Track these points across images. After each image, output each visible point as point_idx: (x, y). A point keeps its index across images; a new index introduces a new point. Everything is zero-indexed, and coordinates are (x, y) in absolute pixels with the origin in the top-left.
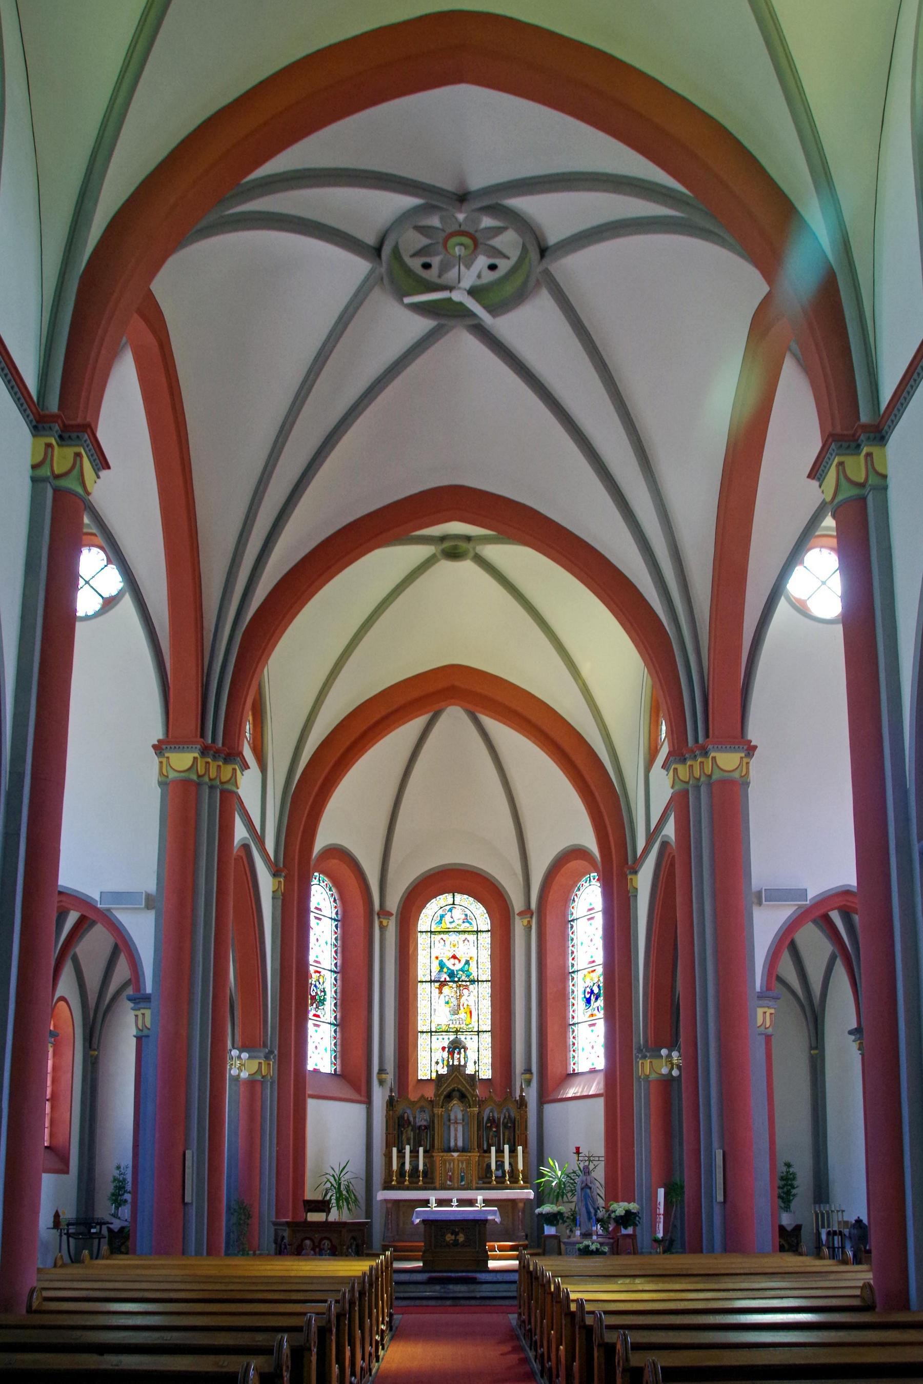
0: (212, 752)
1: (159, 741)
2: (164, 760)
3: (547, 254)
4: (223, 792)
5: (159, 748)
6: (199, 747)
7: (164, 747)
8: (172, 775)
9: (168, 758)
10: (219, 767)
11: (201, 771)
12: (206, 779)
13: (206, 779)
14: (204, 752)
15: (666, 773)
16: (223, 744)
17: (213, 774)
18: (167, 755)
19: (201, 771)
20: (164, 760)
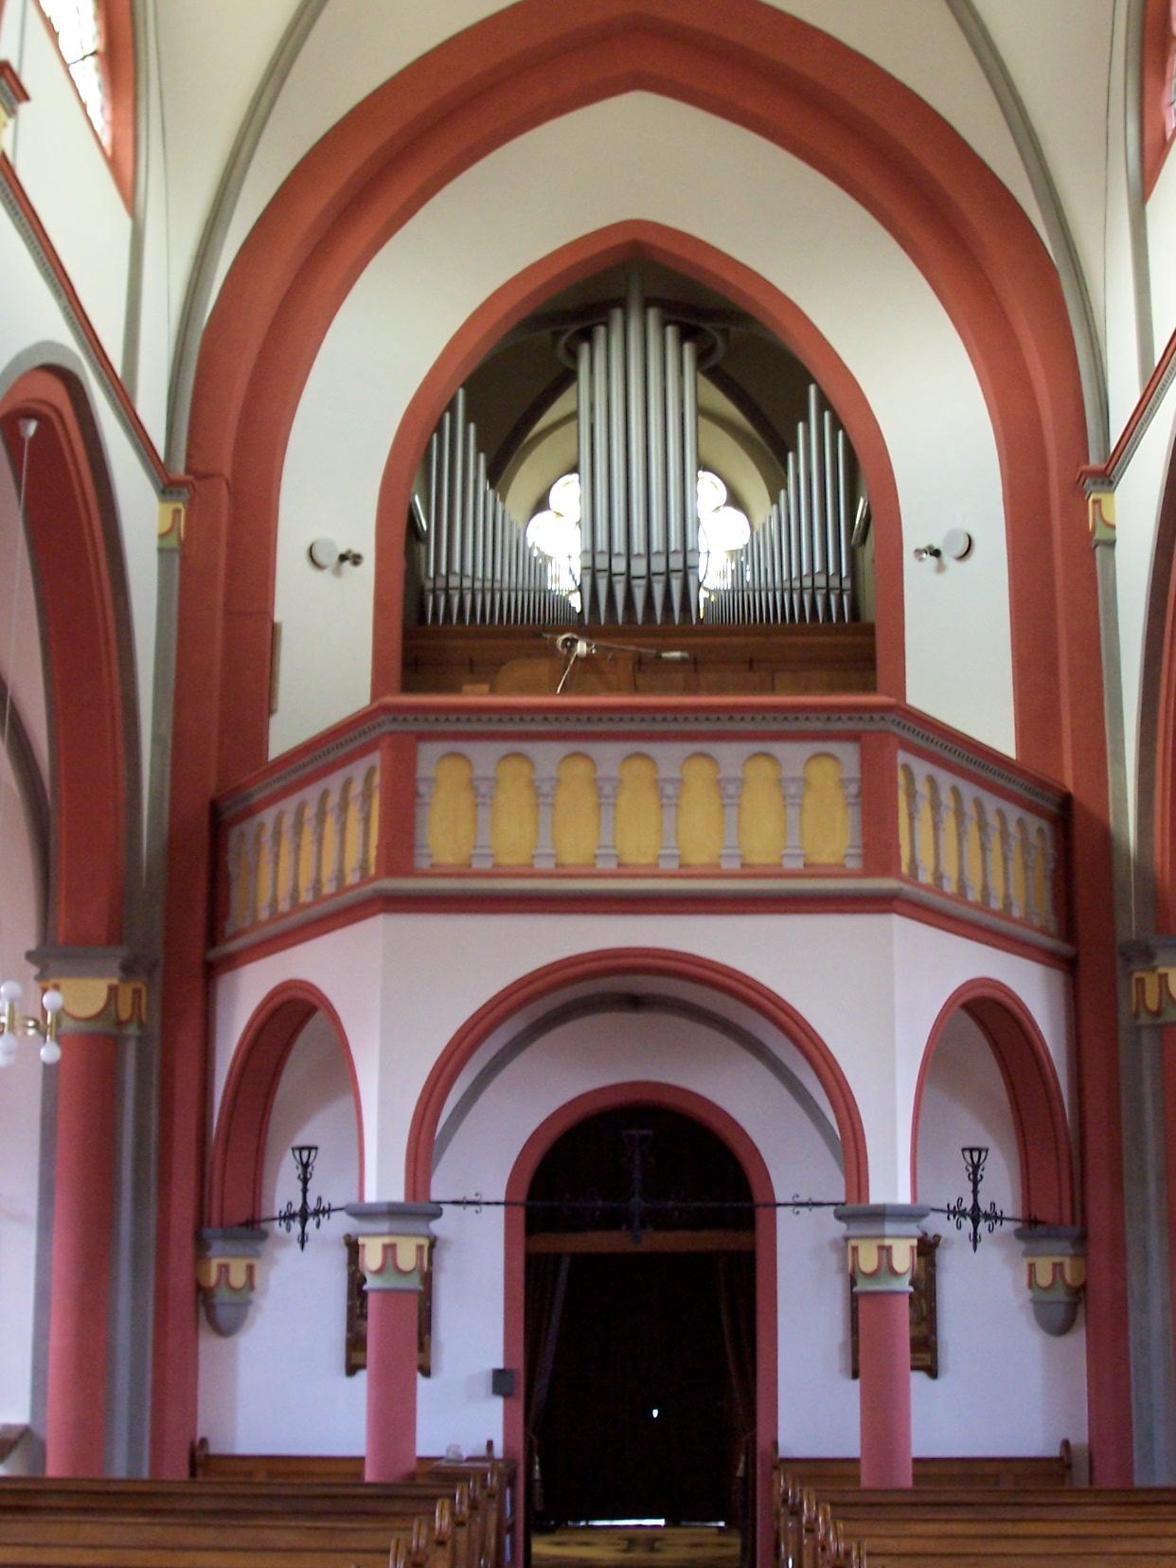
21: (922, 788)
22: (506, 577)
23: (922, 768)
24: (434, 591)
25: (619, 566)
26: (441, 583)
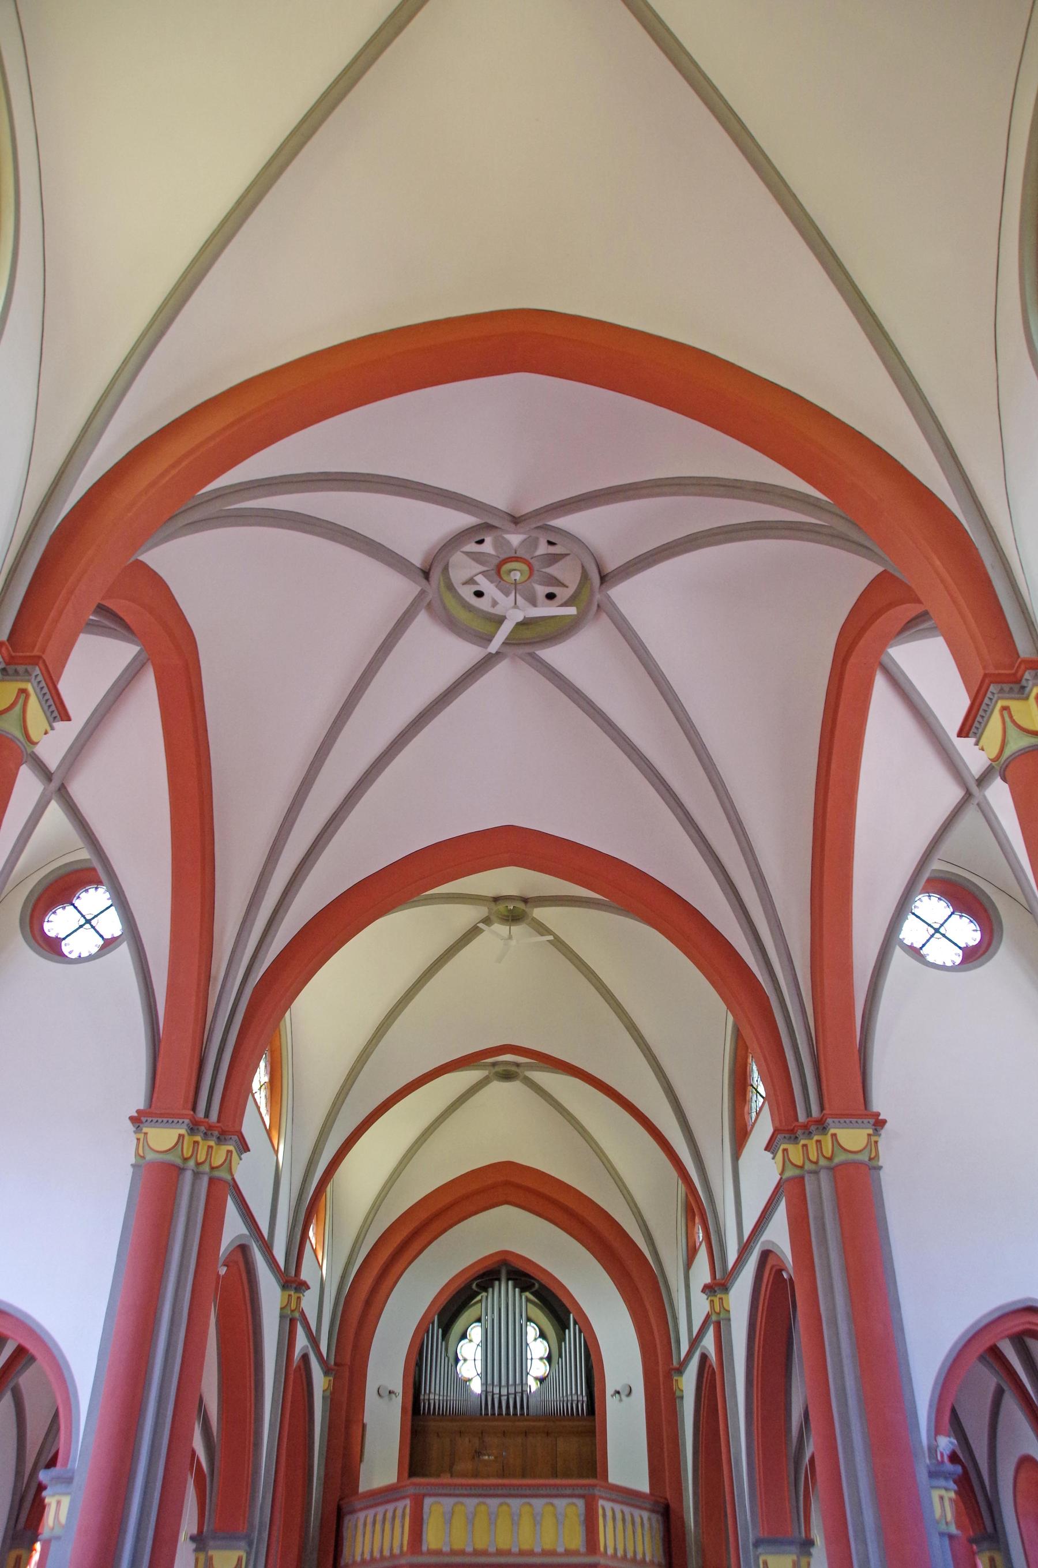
0: (203, 1128)
1: (138, 1111)
2: (141, 1136)
3: (607, 579)
4: (212, 1181)
5: (137, 1120)
6: (187, 1121)
7: (144, 1119)
8: (150, 1156)
9: (146, 1134)
10: (210, 1147)
11: (187, 1153)
12: (191, 1163)
13: (191, 1163)
14: (194, 1128)
15: (771, 1156)
16: (219, 1121)
17: (201, 1157)
18: (145, 1130)
19: (187, 1153)
20: (141, 1136)
21: (609, 1514)
22: (452, 1396)
23: (608, 1505)
24: (424, 1400)
25: (496, 1390)
26: (427, 1397)
